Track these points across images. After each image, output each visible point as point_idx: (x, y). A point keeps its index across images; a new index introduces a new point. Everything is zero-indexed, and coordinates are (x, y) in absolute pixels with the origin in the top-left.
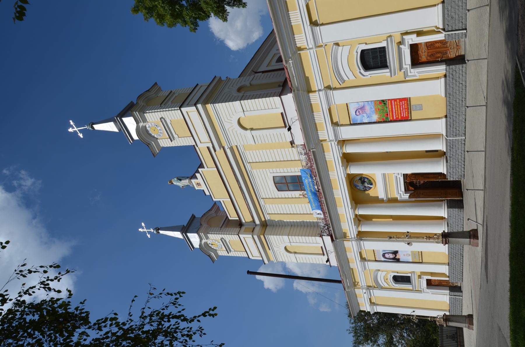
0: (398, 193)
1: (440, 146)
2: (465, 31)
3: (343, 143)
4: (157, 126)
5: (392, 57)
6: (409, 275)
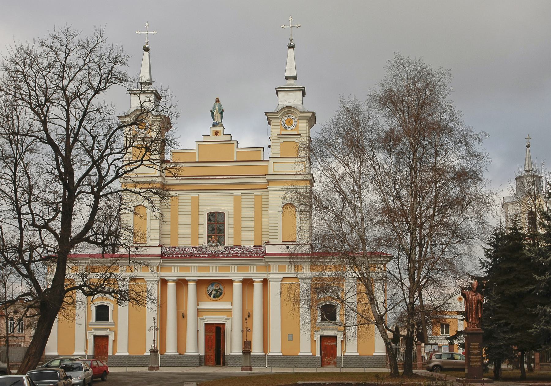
1: (257, 350)
3: (265, 282)
4: (293, 127)
5: (328, 324)
6: (111, 320)
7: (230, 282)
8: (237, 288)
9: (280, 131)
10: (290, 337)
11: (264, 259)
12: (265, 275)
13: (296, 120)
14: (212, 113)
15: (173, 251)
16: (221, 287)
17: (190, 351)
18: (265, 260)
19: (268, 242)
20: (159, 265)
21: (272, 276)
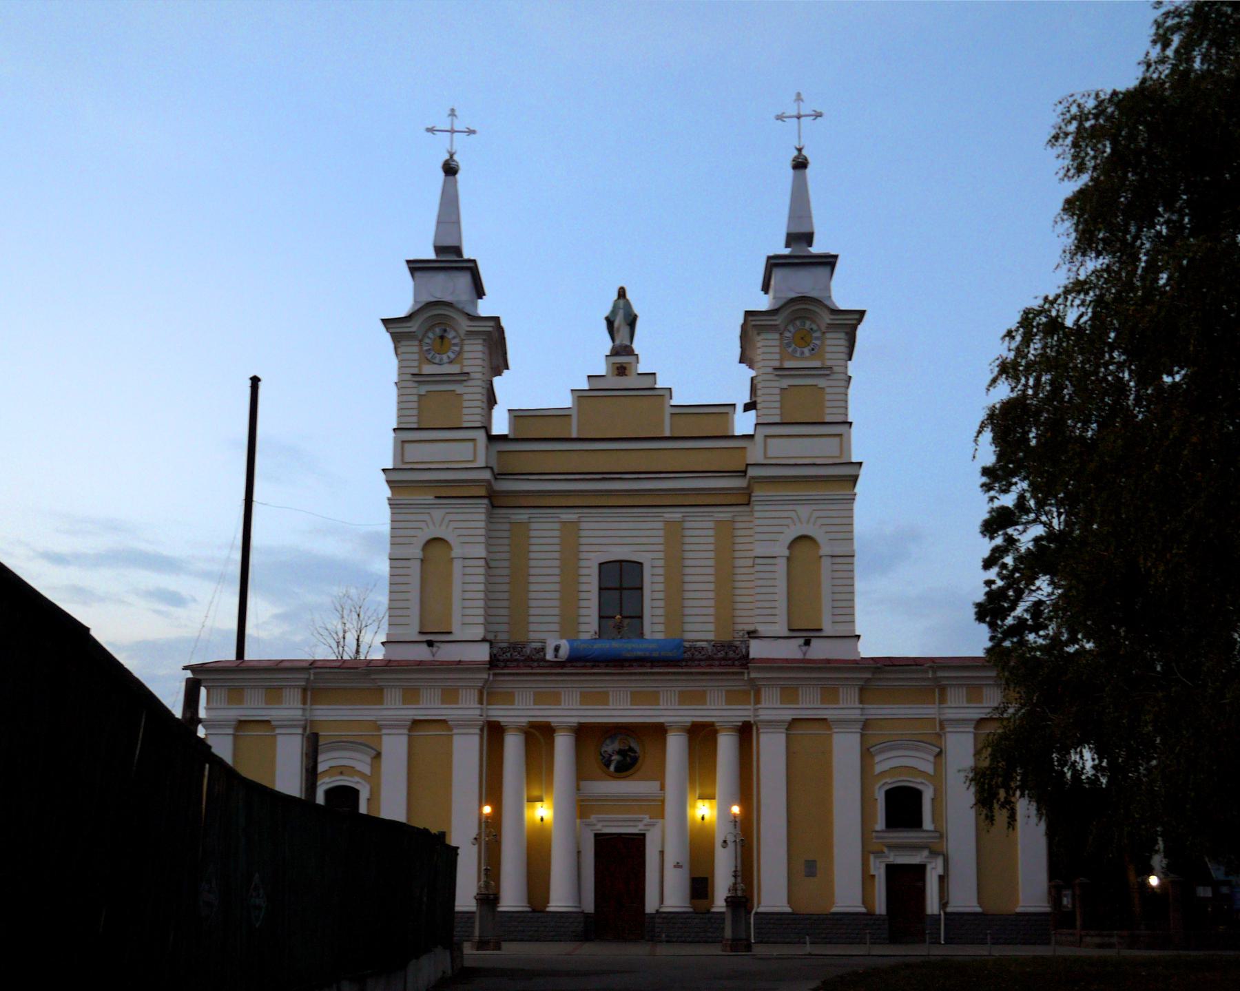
0: (599, 821)
2: (943, 942)
3: (745, 732)
7: (659, 731)
8: (675, 745)
9: (781, 360)
10: (811, 869)
11: (746, 671)
12: (750, 713)
13: (817, 334)
14: (610, 322)
15: (519, 653)
16: (633, 745)
17: (560, 899)
18: (749, 673)
19: (755, 632)
20: (483, 687)
21: (764, 715)
